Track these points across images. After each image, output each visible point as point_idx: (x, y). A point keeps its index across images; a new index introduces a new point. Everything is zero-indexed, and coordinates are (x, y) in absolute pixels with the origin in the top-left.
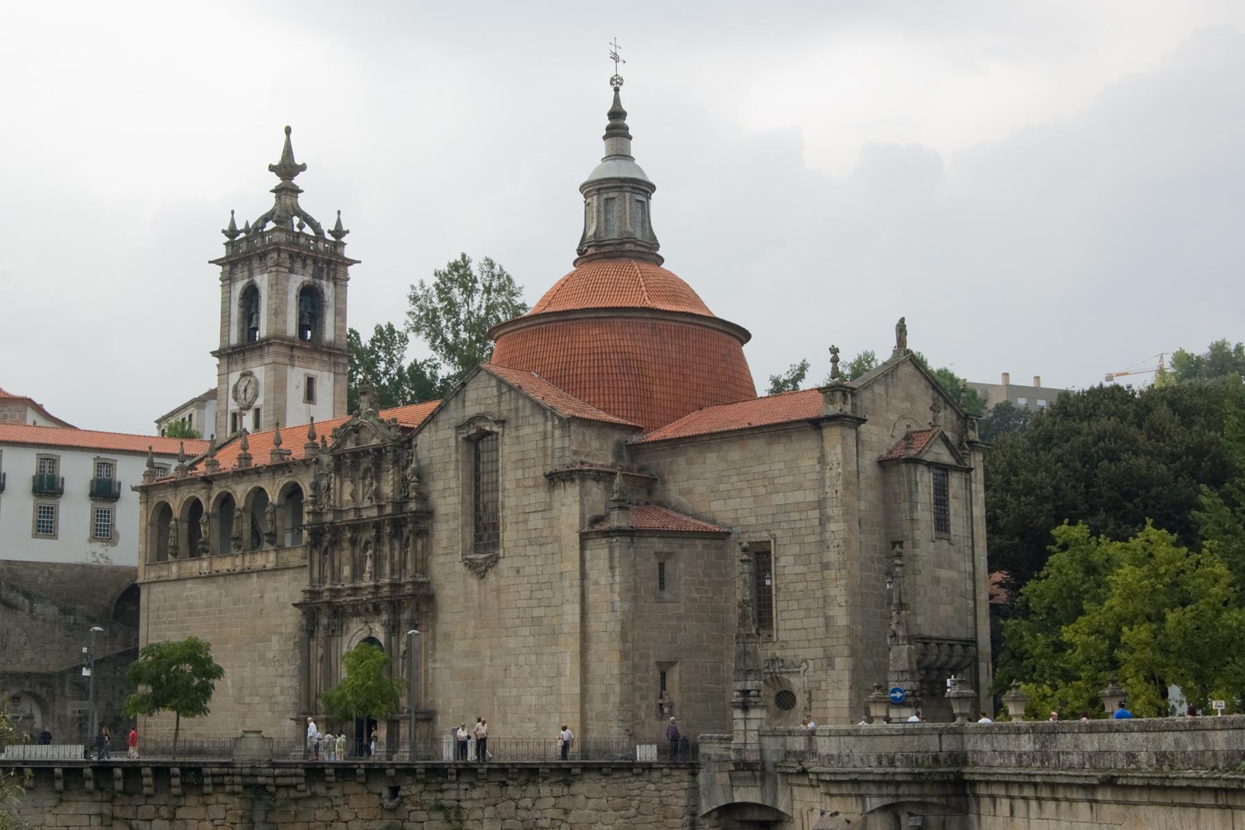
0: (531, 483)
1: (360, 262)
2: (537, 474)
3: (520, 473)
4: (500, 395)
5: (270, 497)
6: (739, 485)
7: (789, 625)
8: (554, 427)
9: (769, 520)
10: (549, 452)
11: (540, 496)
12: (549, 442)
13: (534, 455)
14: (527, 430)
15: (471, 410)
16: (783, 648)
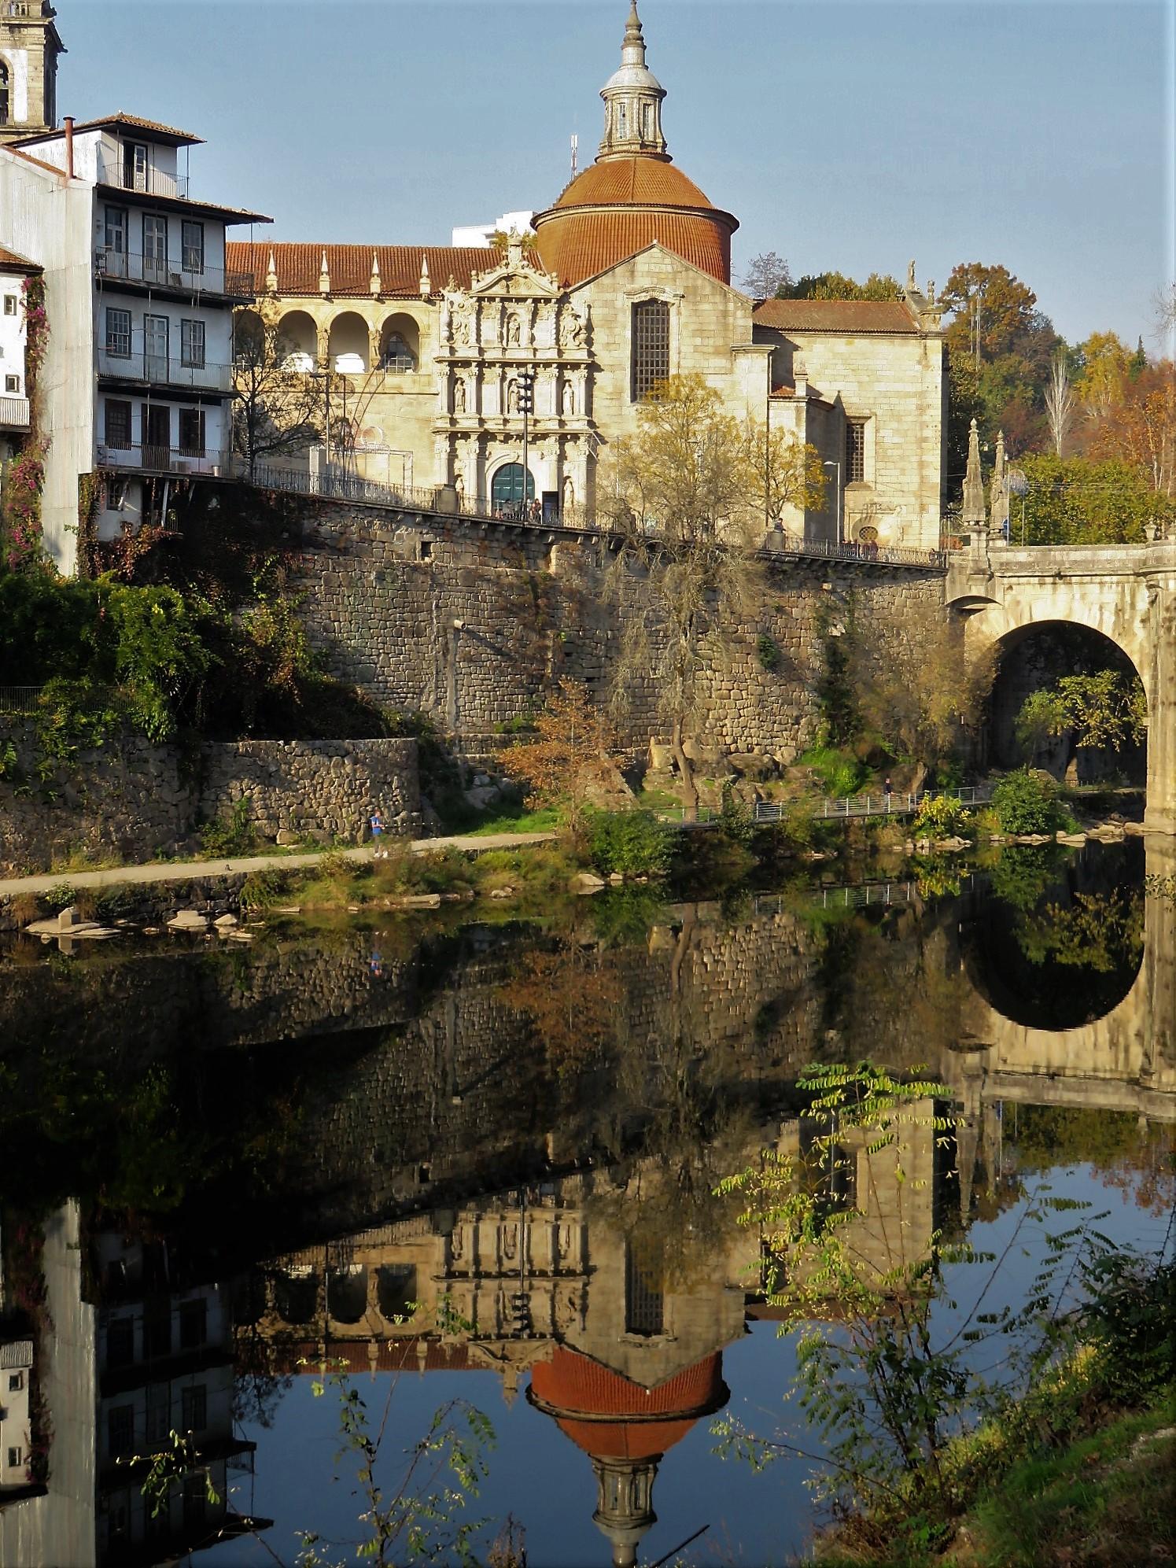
0: (711, 350)
1: (66, 51)
2: (717, 344)
3: (698, 341)
4: (675, 273)
5: (370, 324)
6: (845, 372)
7: (885, 479)
8: (736, 308)
9: (871, 401)
10: (731, 328)
11: (721, 362)
12: (731, 320)
13: (712, 327)
14: (706, 306)
15: (643, 282)
16: (880, 496)
